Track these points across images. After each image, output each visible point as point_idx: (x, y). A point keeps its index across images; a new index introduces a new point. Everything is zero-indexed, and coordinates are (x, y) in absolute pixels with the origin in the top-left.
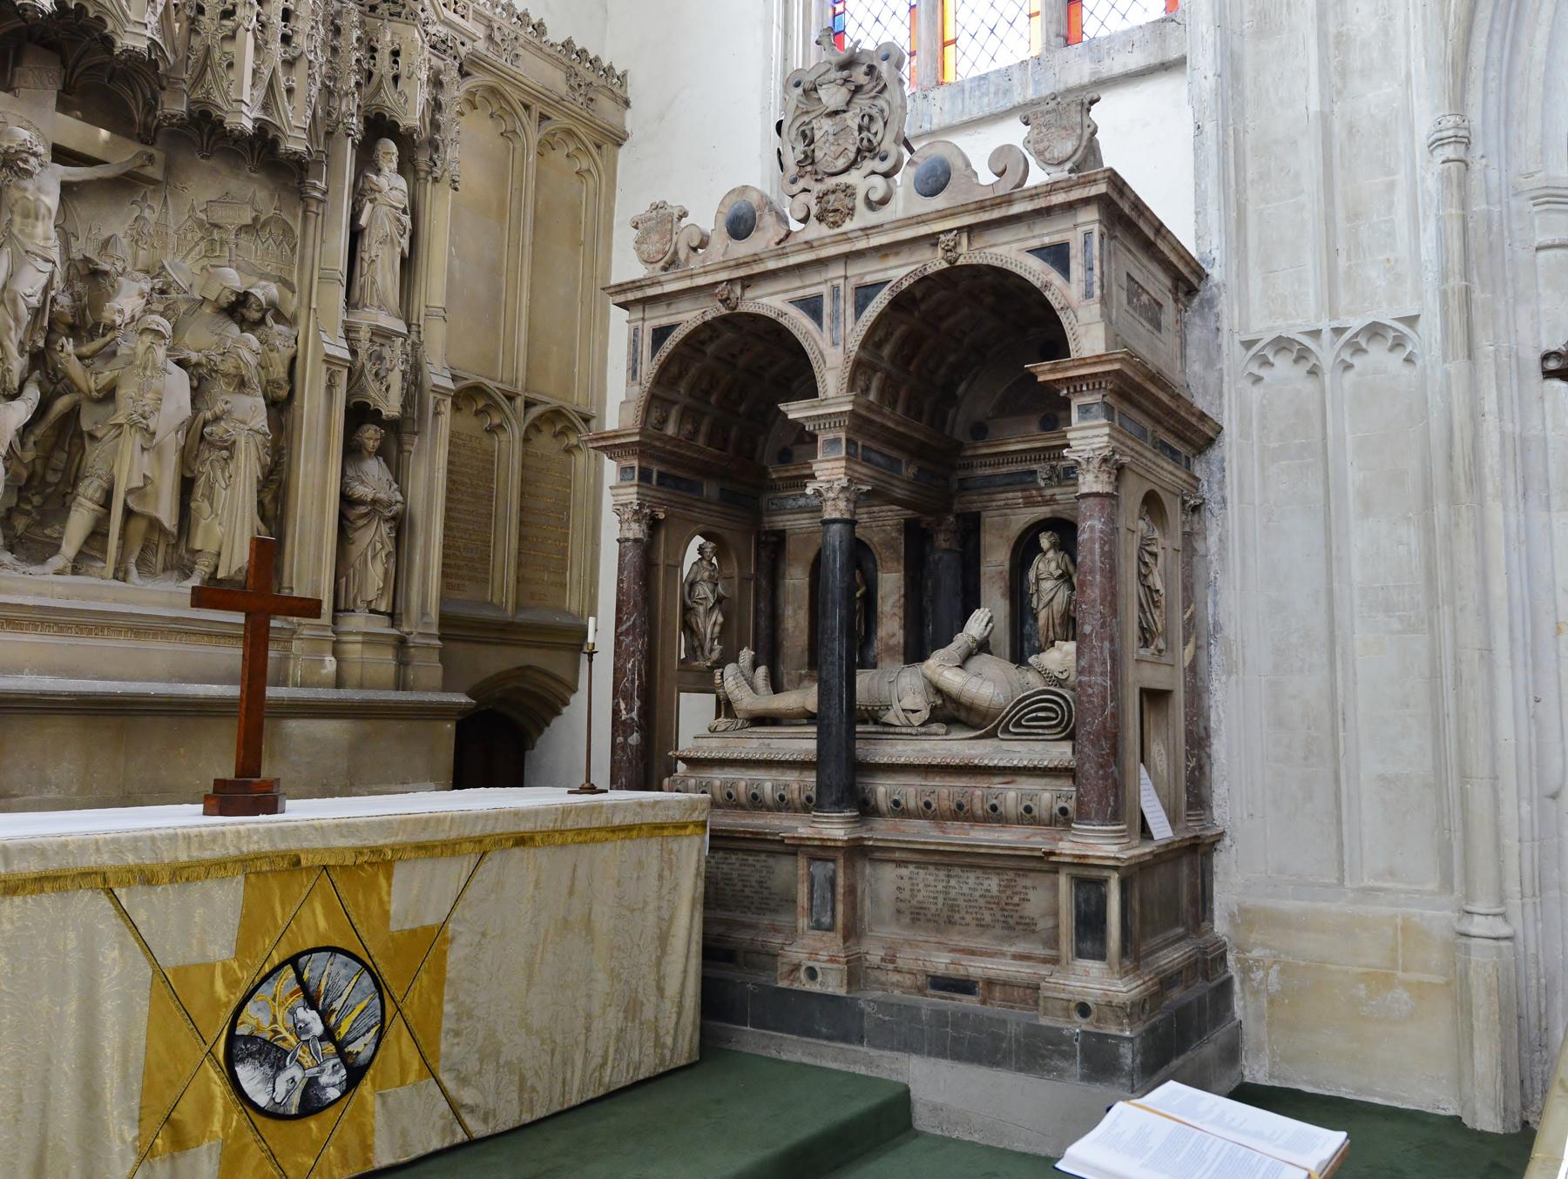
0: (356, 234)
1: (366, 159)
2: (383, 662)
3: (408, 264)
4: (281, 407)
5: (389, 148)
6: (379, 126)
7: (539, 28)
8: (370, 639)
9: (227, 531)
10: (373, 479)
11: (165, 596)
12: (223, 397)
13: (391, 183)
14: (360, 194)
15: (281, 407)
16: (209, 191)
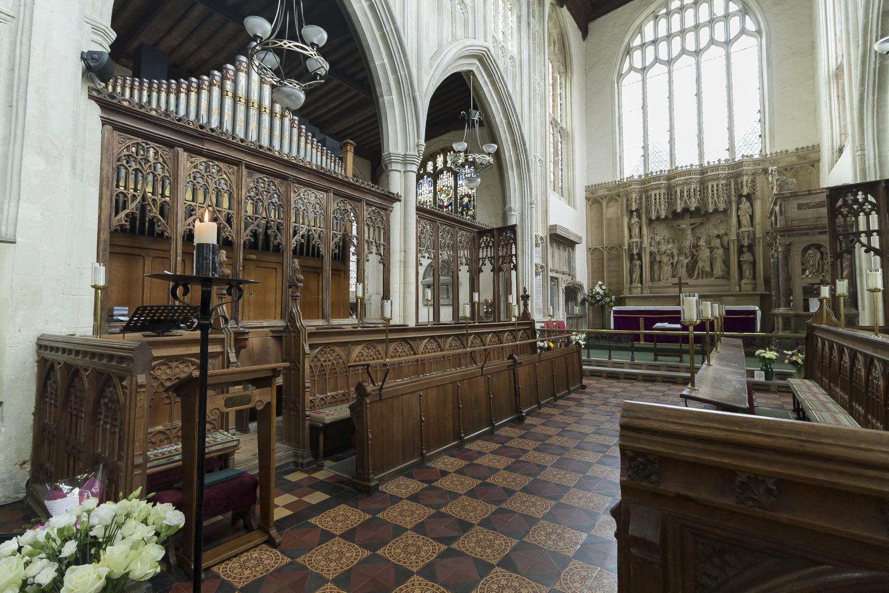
0: (738, 216)
1: (739, 203)
2: (750, 287)
3: (752, 217)
4: (727, 250)
5: (744, 199)
6: (740, 196)
7: (787, 151)
8: (745, 284)
9: (718, 269)
10: (747, 257)
11: (711, 280)
12: (715, 250)
13: (745, 205)
14: (738, 209)
15: (727, 250)
16: (714, 220)
